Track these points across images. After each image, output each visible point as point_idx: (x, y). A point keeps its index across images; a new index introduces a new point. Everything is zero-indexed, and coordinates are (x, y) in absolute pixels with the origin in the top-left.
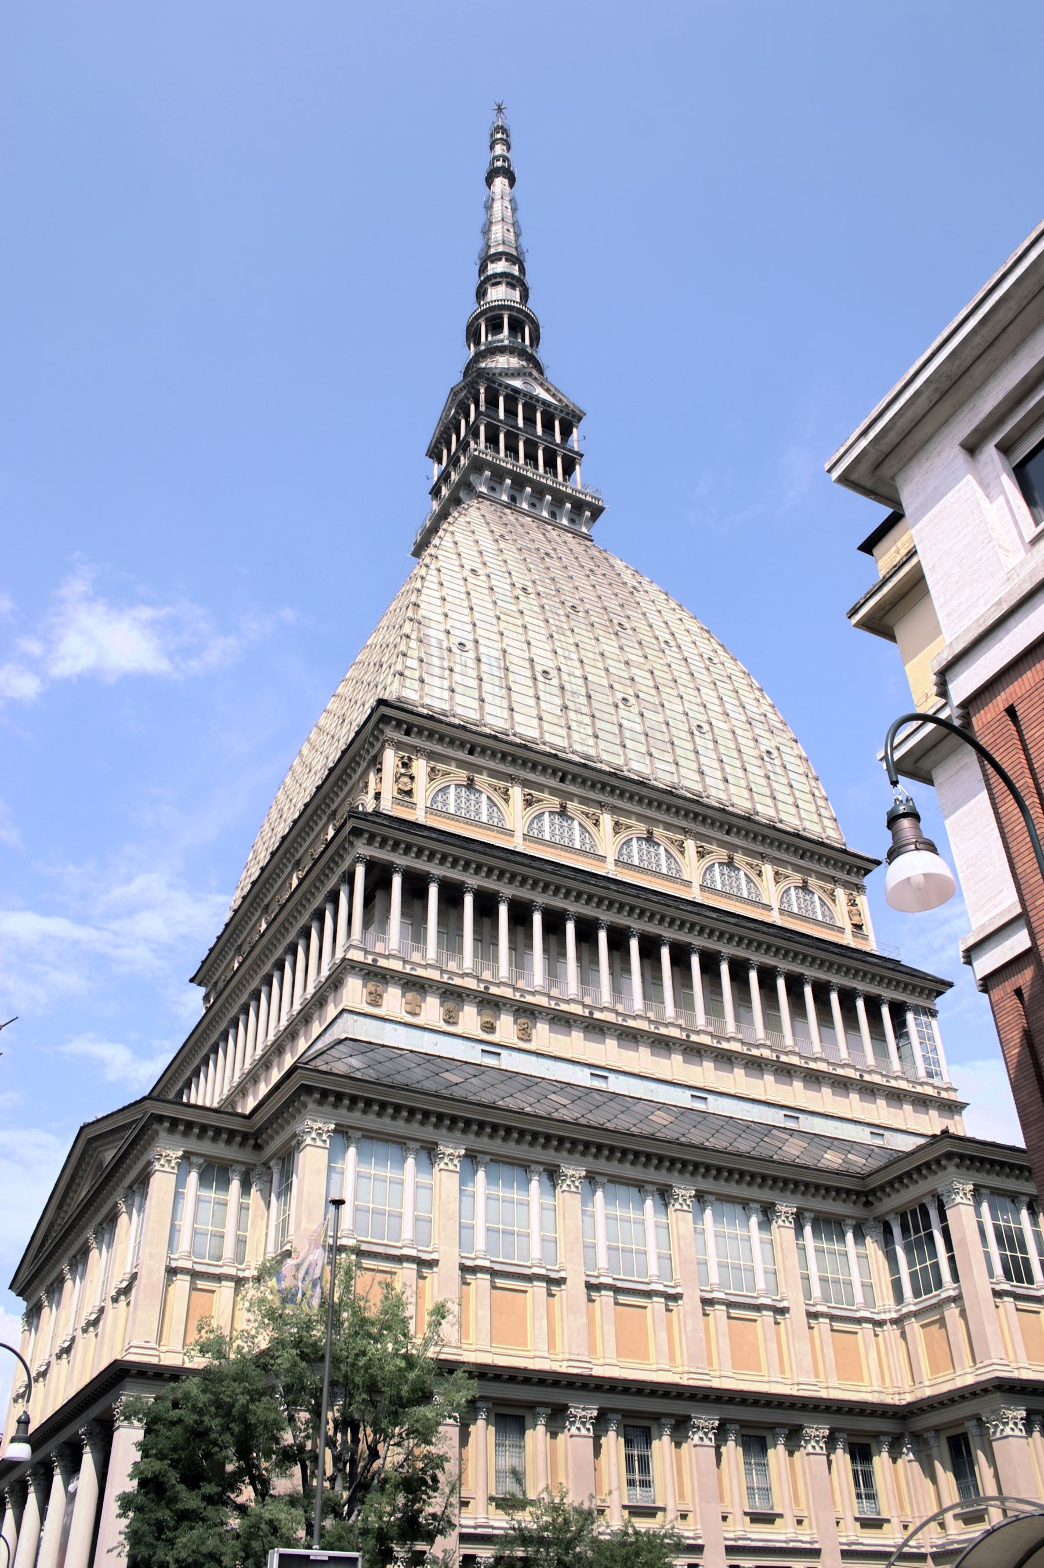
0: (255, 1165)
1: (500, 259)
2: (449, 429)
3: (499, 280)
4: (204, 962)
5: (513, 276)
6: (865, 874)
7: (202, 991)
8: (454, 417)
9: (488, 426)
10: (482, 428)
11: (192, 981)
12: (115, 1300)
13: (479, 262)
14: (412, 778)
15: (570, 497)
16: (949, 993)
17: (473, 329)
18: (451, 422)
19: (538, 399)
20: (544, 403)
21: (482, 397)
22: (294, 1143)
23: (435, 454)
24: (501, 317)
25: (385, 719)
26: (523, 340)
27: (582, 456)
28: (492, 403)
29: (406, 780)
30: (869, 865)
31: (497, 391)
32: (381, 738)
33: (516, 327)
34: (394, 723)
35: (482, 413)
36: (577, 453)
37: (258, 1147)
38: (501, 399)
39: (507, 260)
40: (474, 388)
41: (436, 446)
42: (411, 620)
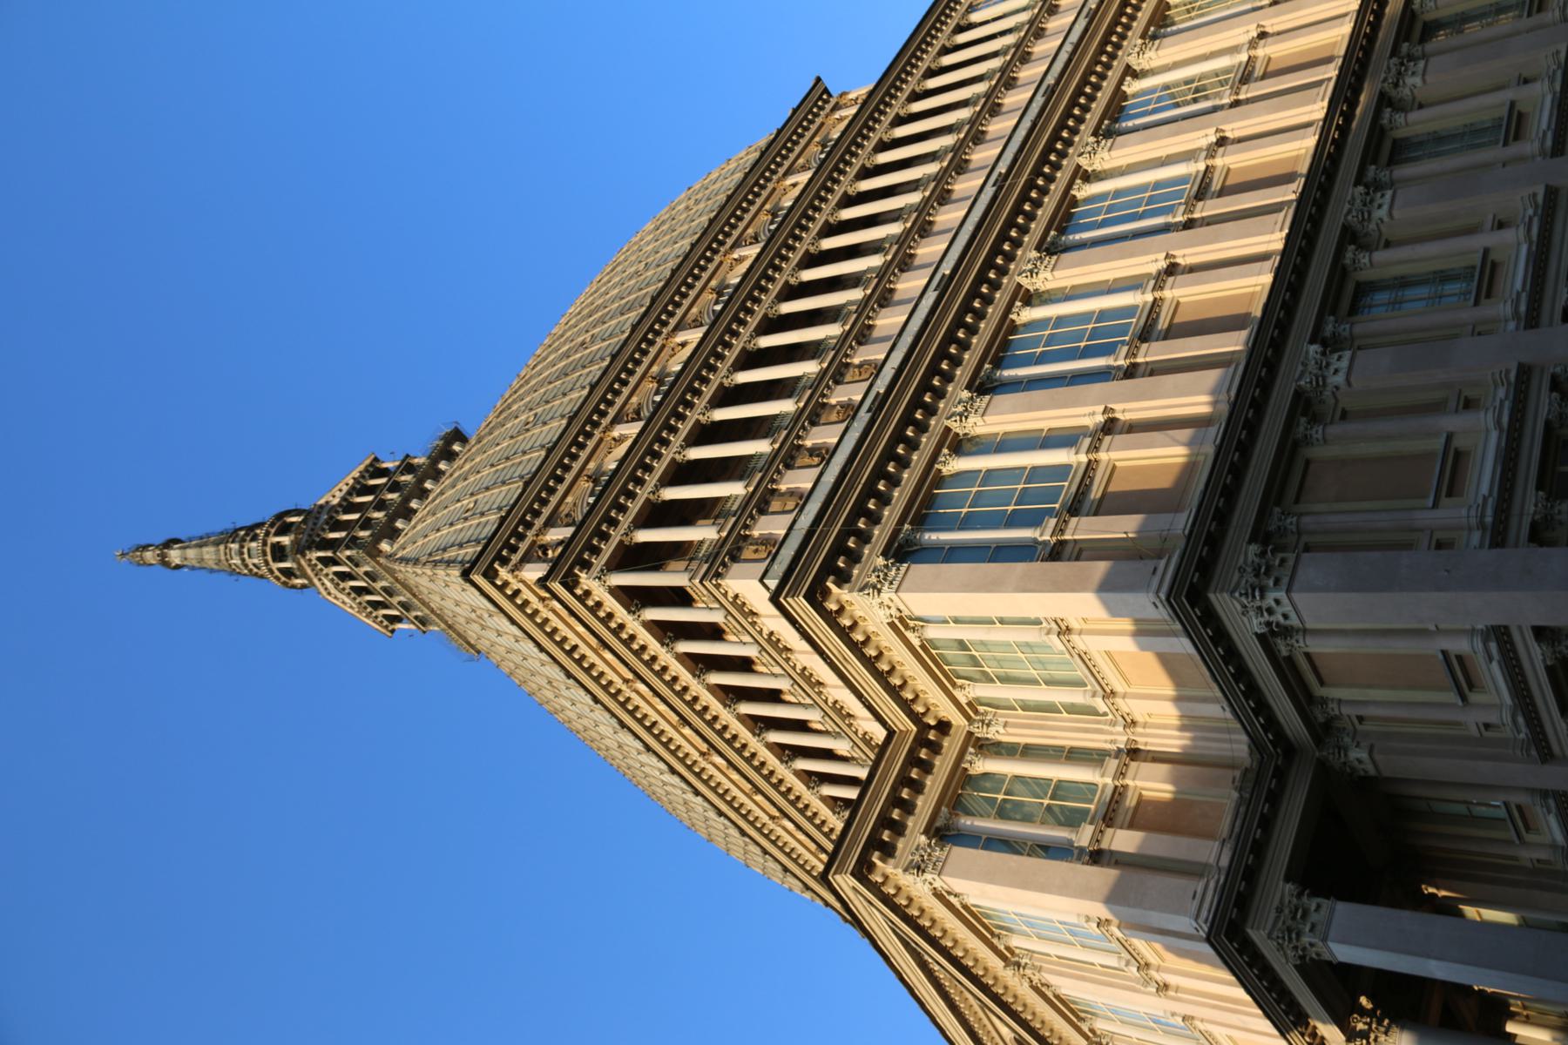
0: (970, 734)
1: (230, 549)
2: (360, 603)
3: (245, 550)
5: (247, 535)
6: (830, 95)
12: (1164, 987)
13: (235, 577)
15: (434, 461)
17: (283, 579)
18: (354, 599)
19: (344, 499)
20: (349, 493)
22: (916, 642)
26: (293, 523)
27: (407, 456)
28: (333, 545)
31: (324, 538)
32: (515, 585)
33: (284, 530)
37: (944, 727)
39: (233, 542)
42: (424, 564)
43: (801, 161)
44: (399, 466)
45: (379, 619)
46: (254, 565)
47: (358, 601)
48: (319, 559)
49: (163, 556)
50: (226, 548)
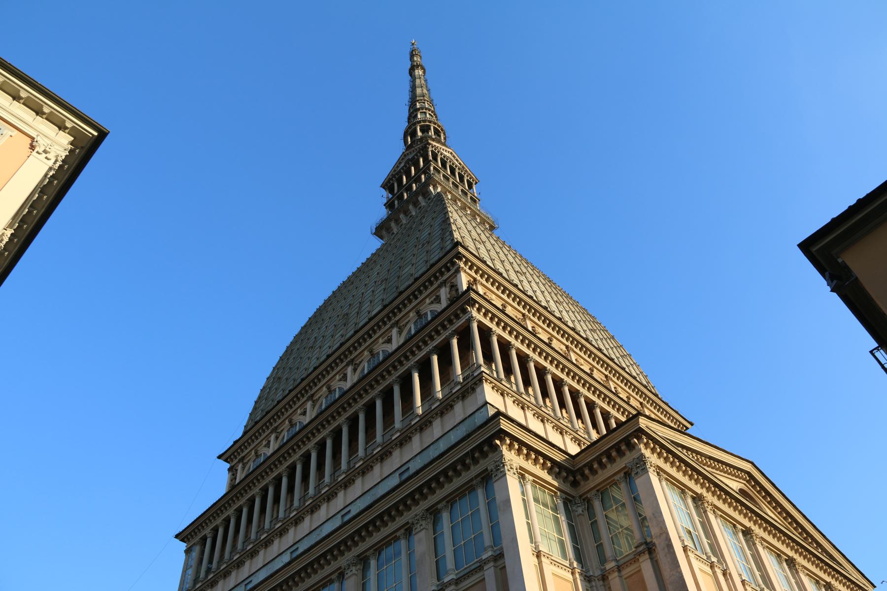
4: (235, 442)
7: (228, 466)
8: (405, 166)
17: (410, 130)
19: (456, 166)
23: (387, 185)
24: (428, 128)
33: (437, 132)
35: (431, 161)
41: (389, 182)
44: (474, 196)
45: (391, 181)
46: (416, 115)
47: (402, 171)
48: (427, 151)
49: (418, 66)
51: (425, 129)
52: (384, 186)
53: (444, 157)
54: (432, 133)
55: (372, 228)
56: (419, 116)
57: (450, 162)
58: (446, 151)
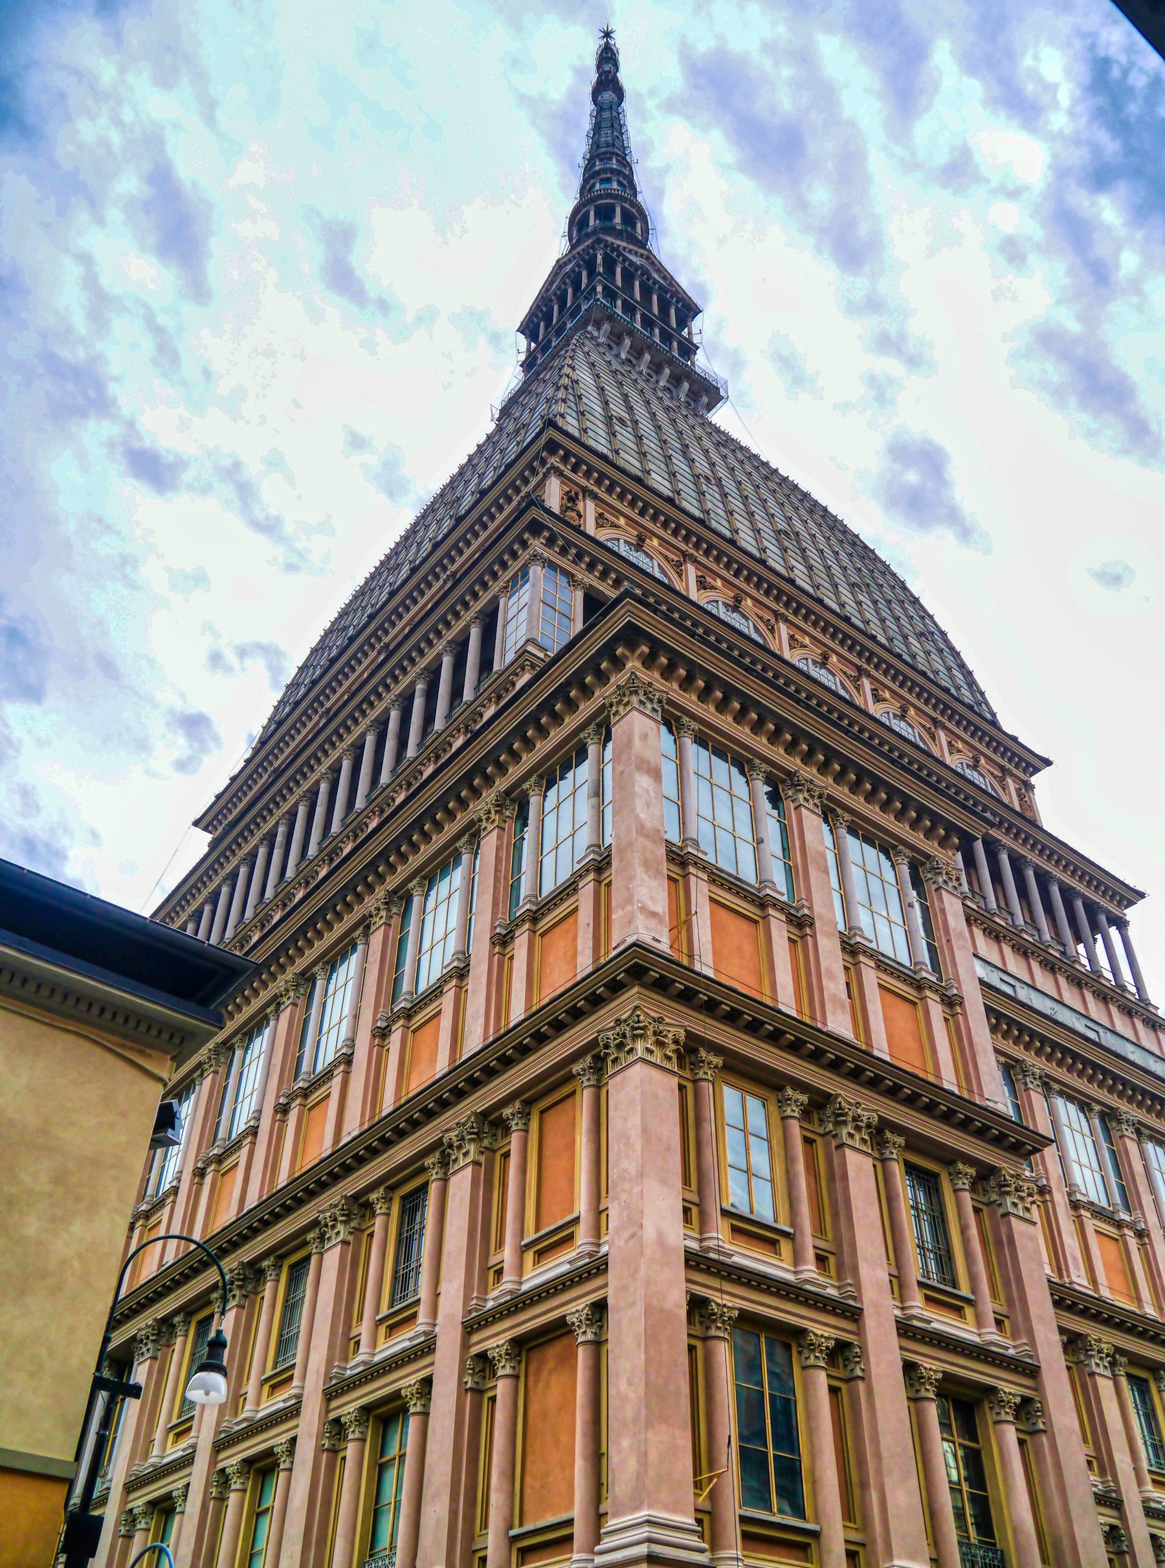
2: (551, 300)
4: (219, 797)
5: (625, 176)
6: (1032, 774)
7: (208, 837)
8: (559, 288)
9: (605, 288)
10: (599, 289)
11: (196, 823)
14: (580, 516)
16: (1141, 903)
18: (555, 294)
19: (655, 282)
20: (661, 287)
21: (599, 258)
23: (529, 328)
25: (552, 447)
27: (698, 348)
29: (574, 514)
30: (1037, 763)
33: (628, 219)
34: (561, 452)
35: (599, 274)
36: (692, 343)
38: (619, 270)
40: (588, 254)
43: (960, 745)
46: (593, 185)
48: (595, 256)
50: (613, 153)
51: (605, 214)
52: (522, 330)
53: (632, 263)
54: (618, 219)
55: (494, 410)
56: (598, 186)
57: (642, 275)
58: (636, 254)
